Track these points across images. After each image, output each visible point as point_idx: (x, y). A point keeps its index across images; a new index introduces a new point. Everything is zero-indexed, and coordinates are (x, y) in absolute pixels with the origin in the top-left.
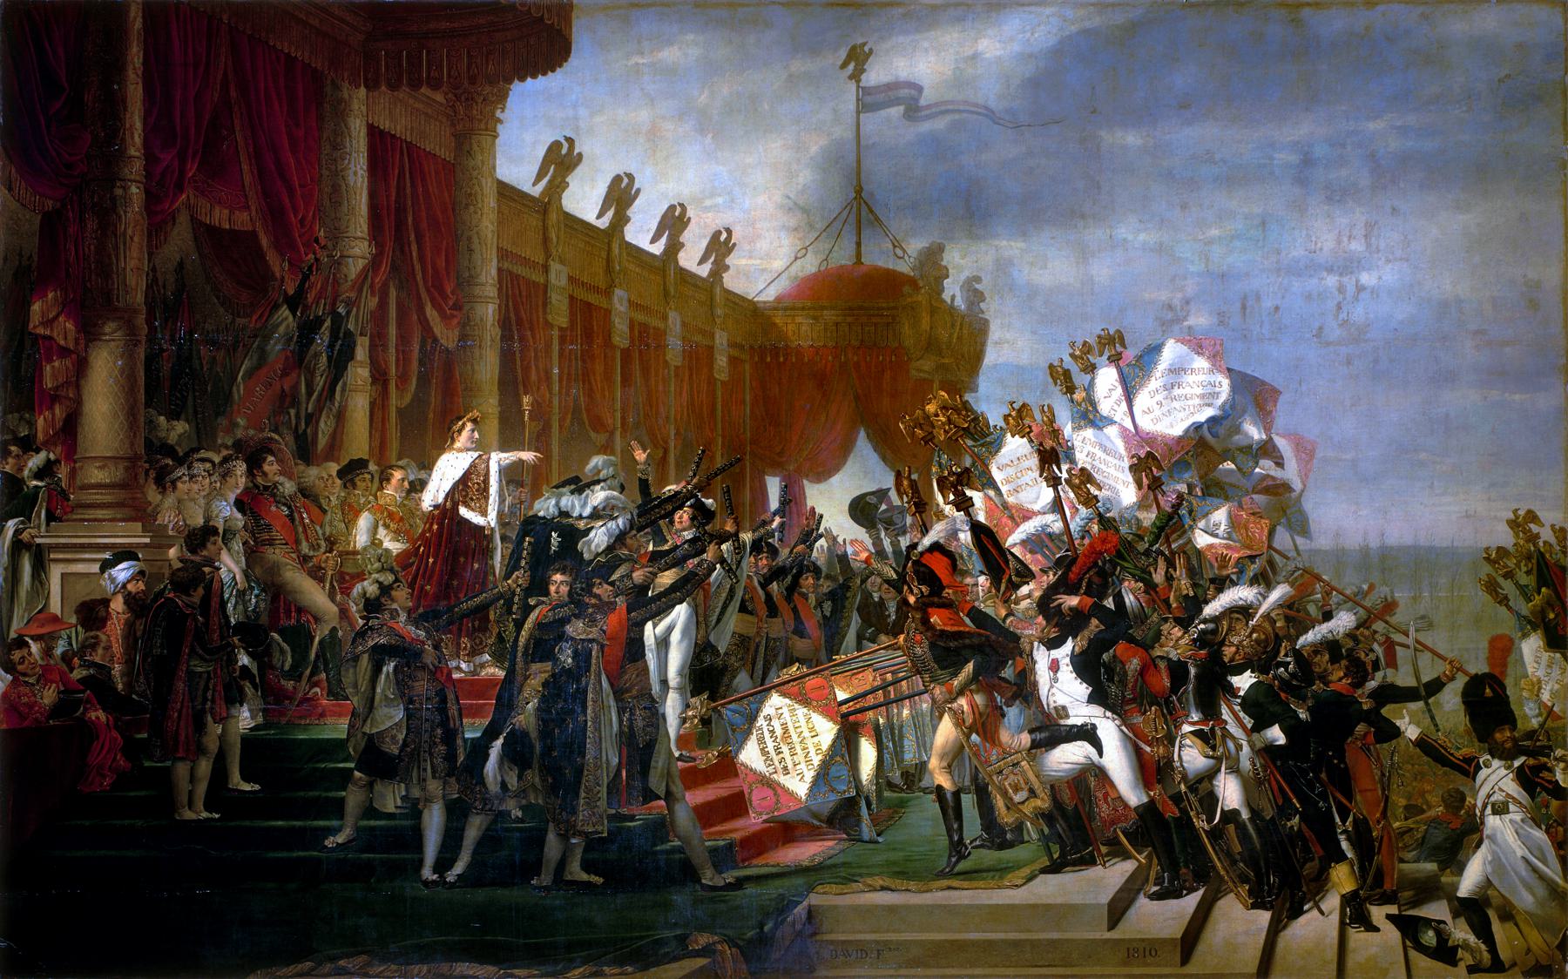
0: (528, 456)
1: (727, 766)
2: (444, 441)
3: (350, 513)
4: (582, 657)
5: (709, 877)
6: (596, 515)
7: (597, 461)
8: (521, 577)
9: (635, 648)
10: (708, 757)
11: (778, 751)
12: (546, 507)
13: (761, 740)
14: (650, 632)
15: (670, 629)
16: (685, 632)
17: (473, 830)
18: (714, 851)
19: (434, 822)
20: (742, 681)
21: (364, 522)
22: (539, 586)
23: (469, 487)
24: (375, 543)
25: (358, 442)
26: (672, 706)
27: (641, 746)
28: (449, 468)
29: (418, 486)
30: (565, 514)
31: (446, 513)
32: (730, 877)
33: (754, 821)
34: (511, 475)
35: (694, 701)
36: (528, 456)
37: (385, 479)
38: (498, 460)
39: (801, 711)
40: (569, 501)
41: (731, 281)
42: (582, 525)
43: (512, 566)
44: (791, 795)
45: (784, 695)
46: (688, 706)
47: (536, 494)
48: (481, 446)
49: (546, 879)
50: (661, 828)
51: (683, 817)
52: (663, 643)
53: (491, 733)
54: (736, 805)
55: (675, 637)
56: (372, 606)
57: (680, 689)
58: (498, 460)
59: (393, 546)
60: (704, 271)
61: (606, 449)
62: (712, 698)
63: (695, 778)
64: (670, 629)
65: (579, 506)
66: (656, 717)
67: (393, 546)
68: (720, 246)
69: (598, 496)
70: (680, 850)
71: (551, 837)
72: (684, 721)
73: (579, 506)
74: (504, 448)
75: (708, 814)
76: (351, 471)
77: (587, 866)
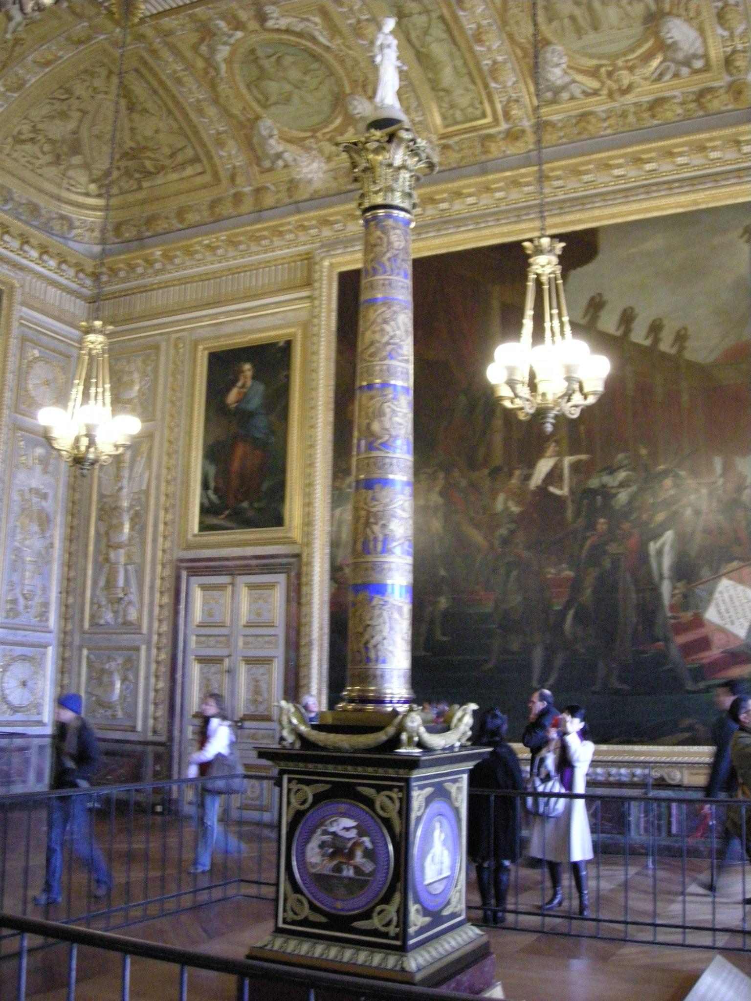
0: (583, 457)
1: (698, 622)
2: (540, 454)
3: (494, 493)
4: (616, 561)
5: (690, 686)
6: (622, 485)
7: (621, 456)
8: (581, 522)
9: (644, 557)
10: (688, 616)
11: (727, 611)
12: (594, 483)
13: (717, 606)
14: (653, 547)
15: (663, 545)
16: (672, 547)
17: (559, 661)
18: (690, 670)
19: (538, 656)
20: (705, 573)
21: (501, 497)
22: (591, 526)
23: (553, 477)
24: (507, 508)
25: (498, 458)
26: (666, 588)
27: (649, 609)
28: (544, 466)
29: (528, 477)
30: (604, 486)
31: (542, 490)
32: (702, 685)
33: (715, 653)
34: (575, 468)
35: (679, 585)
36: (583, 457)
37: (511, 475)
38: (568, 460)
39: (741, 588)
40: (607, 479)
41: (688, 355)
42: (614, 491)
43: (577, 514)
44: (736, 637)
45: (730, 579)
46: (674, 588)
47: (589, 477)
48: (559, 454)
49: (597, 688)
50: (663, 656)
51: (674, 652)
52: (660, 553)
53: (567, 607)
54: (704, 643)
55: (667, 549)
56: (505, 542)
57: (671, 578)
58: (568, 460)
59: (515, 509)
60: (673, 351)
61: (625, 450)
62: (688, 583)
63: (681, 628)
64: (663, 545)
65: (611, 481)
66: (655, 590)
67: (515, 509)
68: (681, 338)
69: (622, 475)
70: (671, 670)
71: (601, 665)
72: (673, 596)
73: (611, 481)
74: (571, 454)
75: (689, 649)
76: (495, 472)
77: (621, 679)
